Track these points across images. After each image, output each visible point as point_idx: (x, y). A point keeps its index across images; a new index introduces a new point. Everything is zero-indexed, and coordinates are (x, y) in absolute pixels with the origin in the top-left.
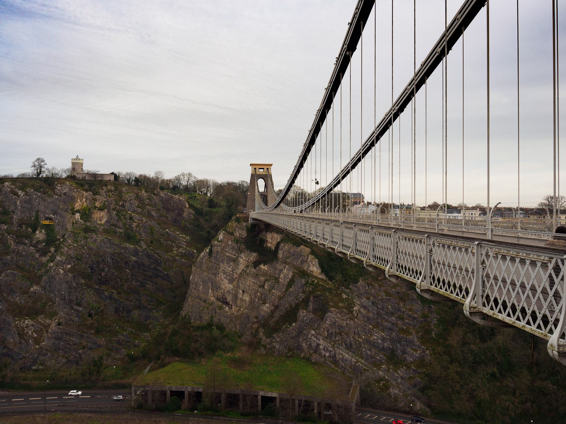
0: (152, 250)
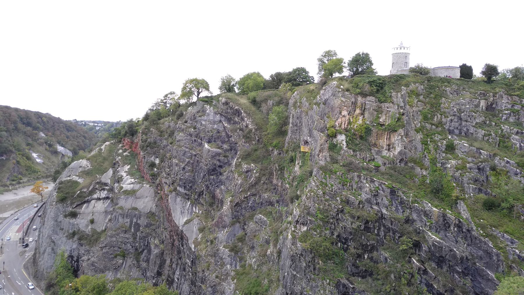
0: (483, 227)
